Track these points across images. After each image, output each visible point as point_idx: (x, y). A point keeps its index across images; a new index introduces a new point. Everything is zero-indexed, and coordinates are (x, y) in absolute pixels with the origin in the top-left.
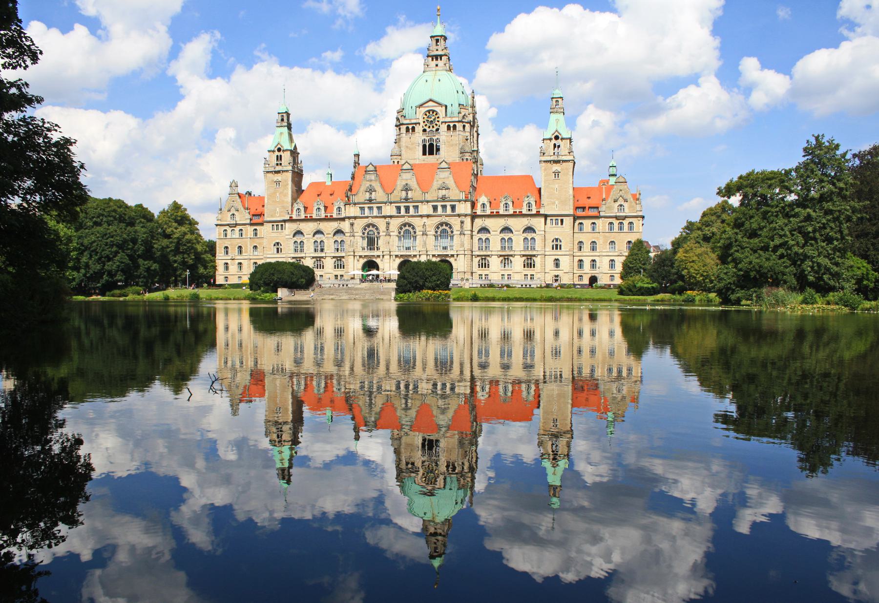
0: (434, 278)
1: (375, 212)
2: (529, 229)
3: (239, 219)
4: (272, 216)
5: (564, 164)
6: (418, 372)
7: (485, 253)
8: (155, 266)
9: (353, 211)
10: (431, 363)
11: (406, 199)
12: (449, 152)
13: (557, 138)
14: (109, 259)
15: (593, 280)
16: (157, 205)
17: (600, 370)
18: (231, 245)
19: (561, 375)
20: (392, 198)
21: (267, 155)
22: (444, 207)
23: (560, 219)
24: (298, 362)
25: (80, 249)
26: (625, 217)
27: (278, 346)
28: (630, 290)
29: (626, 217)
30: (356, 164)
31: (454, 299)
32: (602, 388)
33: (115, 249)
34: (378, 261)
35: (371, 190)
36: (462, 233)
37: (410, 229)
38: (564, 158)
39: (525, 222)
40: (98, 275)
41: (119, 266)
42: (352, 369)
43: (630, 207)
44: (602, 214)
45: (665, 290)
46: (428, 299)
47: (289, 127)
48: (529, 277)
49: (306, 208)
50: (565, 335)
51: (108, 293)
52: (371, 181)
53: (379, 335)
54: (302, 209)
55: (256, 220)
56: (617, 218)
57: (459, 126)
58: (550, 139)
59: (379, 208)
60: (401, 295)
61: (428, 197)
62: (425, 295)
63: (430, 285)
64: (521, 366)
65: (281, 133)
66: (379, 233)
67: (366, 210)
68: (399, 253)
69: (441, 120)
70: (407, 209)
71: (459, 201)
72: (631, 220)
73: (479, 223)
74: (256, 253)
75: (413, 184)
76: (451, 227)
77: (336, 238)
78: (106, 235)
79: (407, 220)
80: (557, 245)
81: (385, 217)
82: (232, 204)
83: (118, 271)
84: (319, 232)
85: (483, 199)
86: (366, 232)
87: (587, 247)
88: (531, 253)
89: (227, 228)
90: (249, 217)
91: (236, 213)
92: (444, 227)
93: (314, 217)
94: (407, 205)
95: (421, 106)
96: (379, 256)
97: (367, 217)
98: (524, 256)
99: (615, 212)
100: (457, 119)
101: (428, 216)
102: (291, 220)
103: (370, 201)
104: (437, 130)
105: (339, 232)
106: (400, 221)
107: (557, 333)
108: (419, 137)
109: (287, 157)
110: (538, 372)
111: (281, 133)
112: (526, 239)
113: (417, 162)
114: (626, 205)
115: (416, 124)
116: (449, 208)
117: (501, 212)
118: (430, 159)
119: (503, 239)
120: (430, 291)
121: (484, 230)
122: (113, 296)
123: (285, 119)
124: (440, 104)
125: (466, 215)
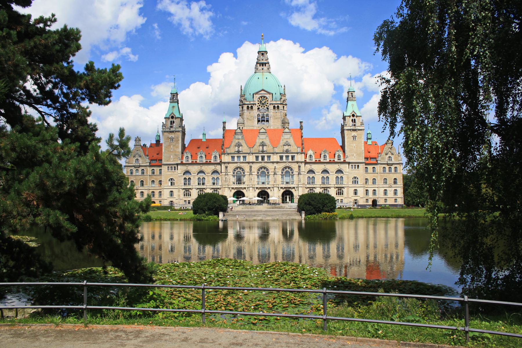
0: (329, 204)
1: (242, 160)
2: (339, 171)
3: (141, 162)
4: (168, 161)
5: (359, 132)
7: (312, 186)
9: (226, 158)
11: (263, 152)
12: (274, 124)
13: (353, 116)
15: (374, 202)
17: (380, 255)
20: (253, 150)
21: (164, 121)
22: (287, 157)
23: (356, 165)
26: (392, 164)
27: (172, 247)
30: (224, 127)
32: (381, 268)
34: (244, 191)
35: (239, 145)
36: (275, 174)
37: (265, 171)
39: (336, 167)
43: (395, 158)
44: (379, 162)
46: (326, 219)
47: (178, 103)
48: (340, 201)
52: (239, 139)
54: (190, 157)
55: (154, 163)
56: (388, 164)
57: (281, 107)
58: (350, 116)
59: (245, 157)
60: (309, 216)
61: (277, 150)
62: (318, 214)
63: (327, 209)
65: (173, 107)
66: (244, 173)
68: (259, 186)
69: (269, 102)
70: (263, 158)
71: (297, 153)
72: (396, 166)
73: (308, 167)
74: (153, 185)
75: (267, 142)
76: (291, 170)
77: (213, 176)
79: (263, 165)
80: (355, 181)
81: (249, 163)
84: (201, 172)
85: (310, 152)
86: (236, 172)
87: (370, 181)
88: (341, 186)
89: (133, 168)
90: (148, 161)
91: (139, 158)
92: (287, 169)
93: (198, 162)
94: (263, 155)
95: (257, 93)
96: (245, 188)
97: (237, 163)
98: (337, 187)
100: (279, 102)
101: (277, 162)
102: (182, 164)
103: (239, 152)
104: (268, 108)
106: (258, 166)
108: (255, 112)
110: (347, 260)
111: (173, 107)
112: (337, 177)
113: (255, 128)
114: (393, 157)
115: (253, 104)
116: (290, 158)
117: (322, 160)
119: (323, 177)
120: (327, 214)
121: (311, 171)
124: (269, 93)
125: (302, 162)
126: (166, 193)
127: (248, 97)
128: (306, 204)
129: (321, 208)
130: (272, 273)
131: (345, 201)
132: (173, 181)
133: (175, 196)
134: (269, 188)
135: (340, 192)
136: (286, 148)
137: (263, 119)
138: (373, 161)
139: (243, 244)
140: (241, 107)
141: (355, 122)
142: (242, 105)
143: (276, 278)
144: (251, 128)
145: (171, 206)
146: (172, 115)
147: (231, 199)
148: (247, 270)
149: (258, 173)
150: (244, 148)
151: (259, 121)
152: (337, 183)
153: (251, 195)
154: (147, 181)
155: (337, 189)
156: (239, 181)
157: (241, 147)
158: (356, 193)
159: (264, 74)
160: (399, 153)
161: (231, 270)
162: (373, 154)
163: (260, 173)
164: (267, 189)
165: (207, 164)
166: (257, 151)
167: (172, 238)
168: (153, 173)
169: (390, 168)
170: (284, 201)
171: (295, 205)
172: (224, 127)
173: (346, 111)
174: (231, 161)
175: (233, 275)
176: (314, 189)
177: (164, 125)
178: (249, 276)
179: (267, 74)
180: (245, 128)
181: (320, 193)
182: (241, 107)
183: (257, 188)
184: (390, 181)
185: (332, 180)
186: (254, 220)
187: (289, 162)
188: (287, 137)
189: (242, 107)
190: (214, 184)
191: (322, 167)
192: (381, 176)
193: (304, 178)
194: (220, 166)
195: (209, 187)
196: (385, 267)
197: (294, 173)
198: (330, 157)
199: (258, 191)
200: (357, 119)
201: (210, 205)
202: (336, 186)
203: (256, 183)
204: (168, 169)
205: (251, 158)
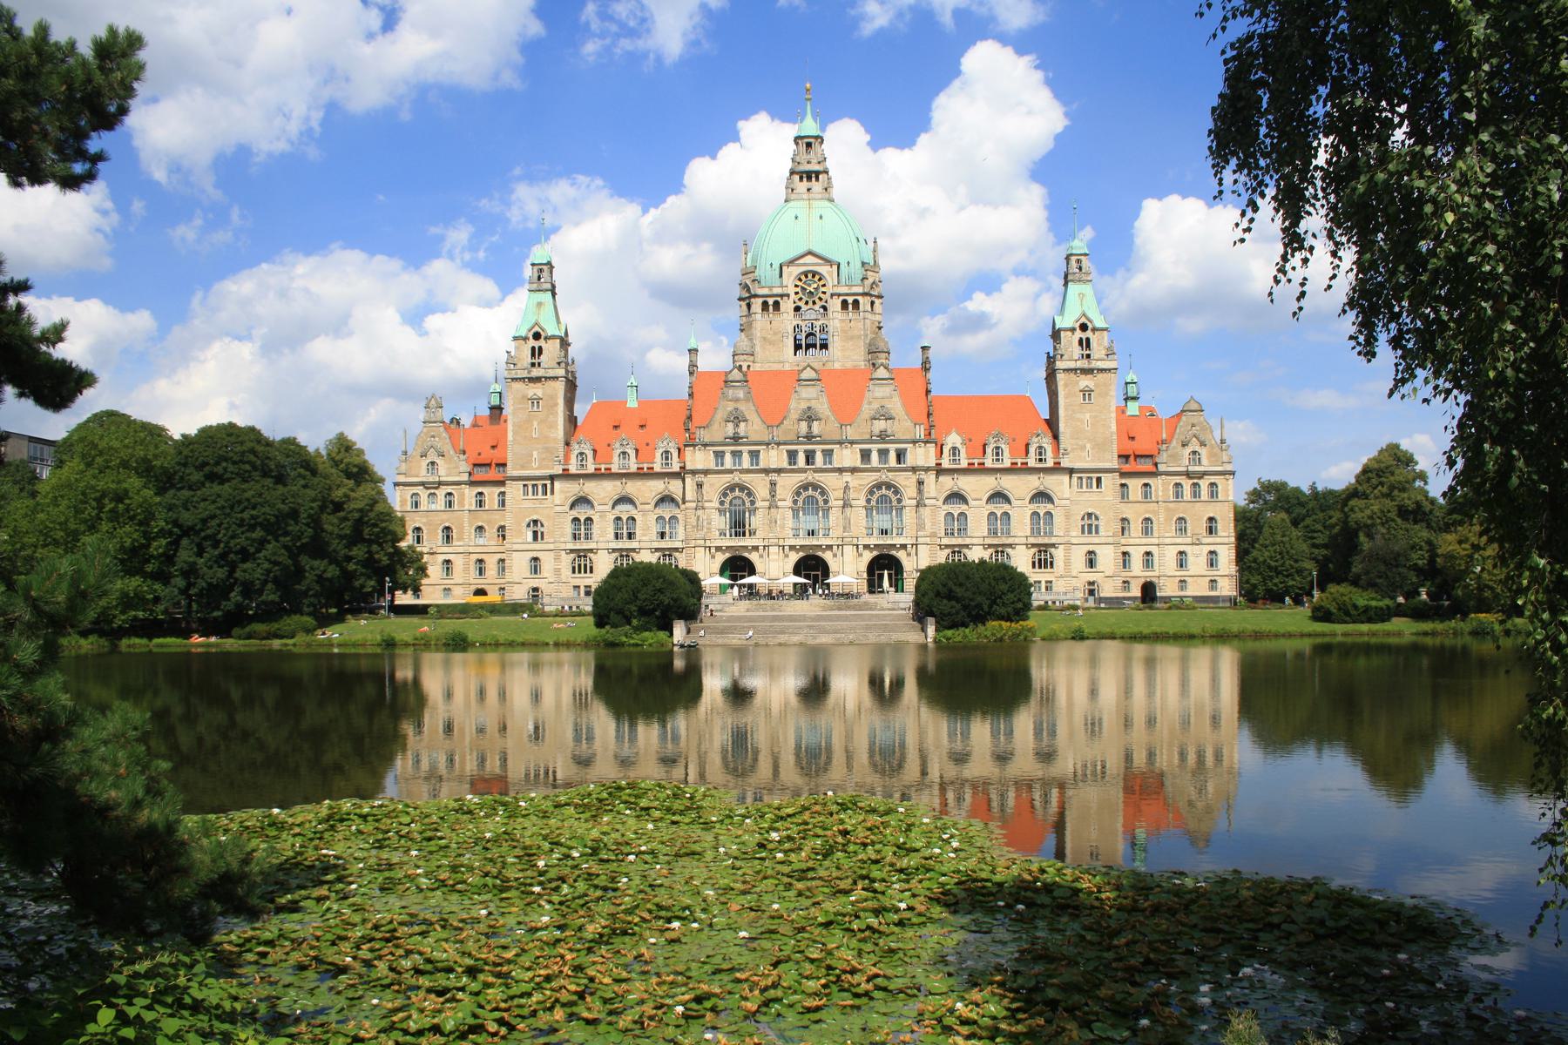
0: (1010, 596)
1: (746, 462)
2: (1042, 496)
3: (443, 473)
4: (523, 467)
5: (1100, 376)
6: (837, 771)
7: (960, 541)
8: (332, 571)
9: (699, 459)
10: (862, 757)
11: (809, 438)
12: (844, 354)
13: (1084, 327)
14: (245, 555)
15: (1149, 590)
16: (315, 440)
18: (428, 524)
19: (1104, 767)
20: (779, 434)
21: (511, 346)
22: (883, 453)
23: (1094, 477)
24: (584, 762)
25: (171, 533)
26: (1202, 475)
27: (536, 728)
28: (1347, 613)
29: (1205, 473)
30: (693, 366)
31: (1043, 639)
33: (258, 533)
34: (753, 557)
35: (737, 419)
37: (817, 495)
38: (1101, 365)
39: (1033, 483)
40: (217, 592)
41: (269, 571)
42: (702, 776)
43: (1211, 455)
44: (1162, 468)
45: (1399, 612)
46: (1001, 640)
47: (554, 294)
50: (1109, 692)
51: (236, 631)
52: (737, 400)
53: (758, 700)
54: (590, 454)
55: (481, 474)
56: (1188, 475)
57: (864, 302)
58: (1073, 330)
59: (755, 455)
60: (949, 633)
61: (851, 433)
62: (977, 630)
63: (1003, 611)
64: (1031, 756)
65: (540, 304)
66: (753, 503)
67: (728, 458)
70: (810, 457)
71: (914, 442)
72: (1213, 479)
73: (948, 483)
74: (481, 541)
75: (823, 407)
76: (897, 492)
77: (659, 511)
78: (240, 502)
79: (810, 477)
80: (1090, 526)
81: (767, 471)
82: (430, 442)
83: (265, 582)
85: (953, 439)
87: (1136, 527)
88: (1046, 541)
91: (439, 461)
92: (884, 491)
93: (615, 469)
94: (809, 448)
95: (792, 262)
96: (756, 548)
97: (730, 471)
98: (1033, 545)
99: (1184, 464)
100: (860, 290)
101: (853, 470)
102: (566, 476)
103: (736, 439)
104: (825, 308)
105: (666, 499)
106: (795, 480)
107: (1093, 692)
108: (787, 320)
110: (1066, 764)
111: (540, 304)
112: (1035, 514)
113: (787, 367)
114: (1203, 452)
115: (782, 296)
116: (892, 456)
117: (989, 463)
119: (992, 514)
120: (1005, 624)
121: (956, 497)
122: (249, 637)
123: (546, 274)
125: (927, 470)
126: (519, 565)
127: (766, 273)
128: (938, 594)
129: (986, 608)
130: (792, 844)
131: (1059, 586)
132: (539, 528)
133: (544, 574)
134: (830, 547)
135: (1043, 560)
136: (880, 425)
137: (809, 342)
138: (1146, 466)
139: (751, 717)
140: (744, 304)
141: (1088, 346)
142: (747, 299)
143: (804, 866)
144: (776, 367)
145: (532, 606)
146: (537, 329)
147: (711, 579)
148: (707, 826)
149: (795, 502)
150: (753, 428)
151: (797, 347)
152: (1035, 531)
153: (775, 570)
154: (461, 528)
155: (1034, 550)
156: (739, 526)
157: (742, 425)
158: (1091, 563)
159: (815, 204)
160: (1223, 441)
161: (650, 826)
162: (1141, 446)
163: (800, 503)
164: (824, 551)
165: (640, 475)
166: (792, 437)
167: (536, 697)
168: (481, 503)
169: (1195, 485)
170: (874, 586)
171: (907, 598)
172: (693, 366)
173: (1062, 311)
174: (712, 466)
175: (652, 852)
176: (965, 551)
177: (511, 361)
178: (709, 855)
179: (822, 206)
180: (756, 367)
181: (982, 562)
182: (744, 304)
183: (792, 548)
184: (1197, 526)
185: (1021, 525)
186: (780, 644)
187: (890, 470)
188: (882, 394)
189: (749, 306)
190: (662, 535)
191: (988, 483)
192: (1168, 509)
193: (935, 516)
194: (679, 483)
195: (648, 545)
196: (1181, 787)
197: (906, 502)
198: (1012, 454)
199: (794, 557)
200: (1094, 338)
201: (646, 601)
202: (1032, 540)
203: (791, 533)
204: (526, 493)
205: (774, 458)
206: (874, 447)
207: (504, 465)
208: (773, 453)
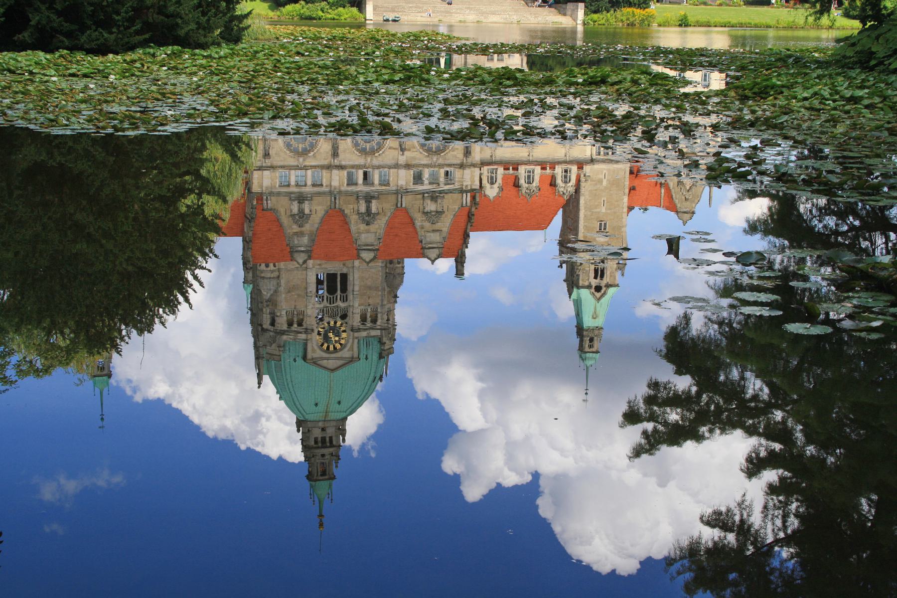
30: (460, 261)
49: (553, 184)
54: (559, 181)
95: (352, 360)
102: (580, 165)
109: (587, 277)
115: (359, 330)
118: (335, 267)
124: (315, 362)
146: (598, 295)
177: (621, 267)
179: (314, 414)
206: (309, 189)
207: (631, 173)
208: (402, 182)
